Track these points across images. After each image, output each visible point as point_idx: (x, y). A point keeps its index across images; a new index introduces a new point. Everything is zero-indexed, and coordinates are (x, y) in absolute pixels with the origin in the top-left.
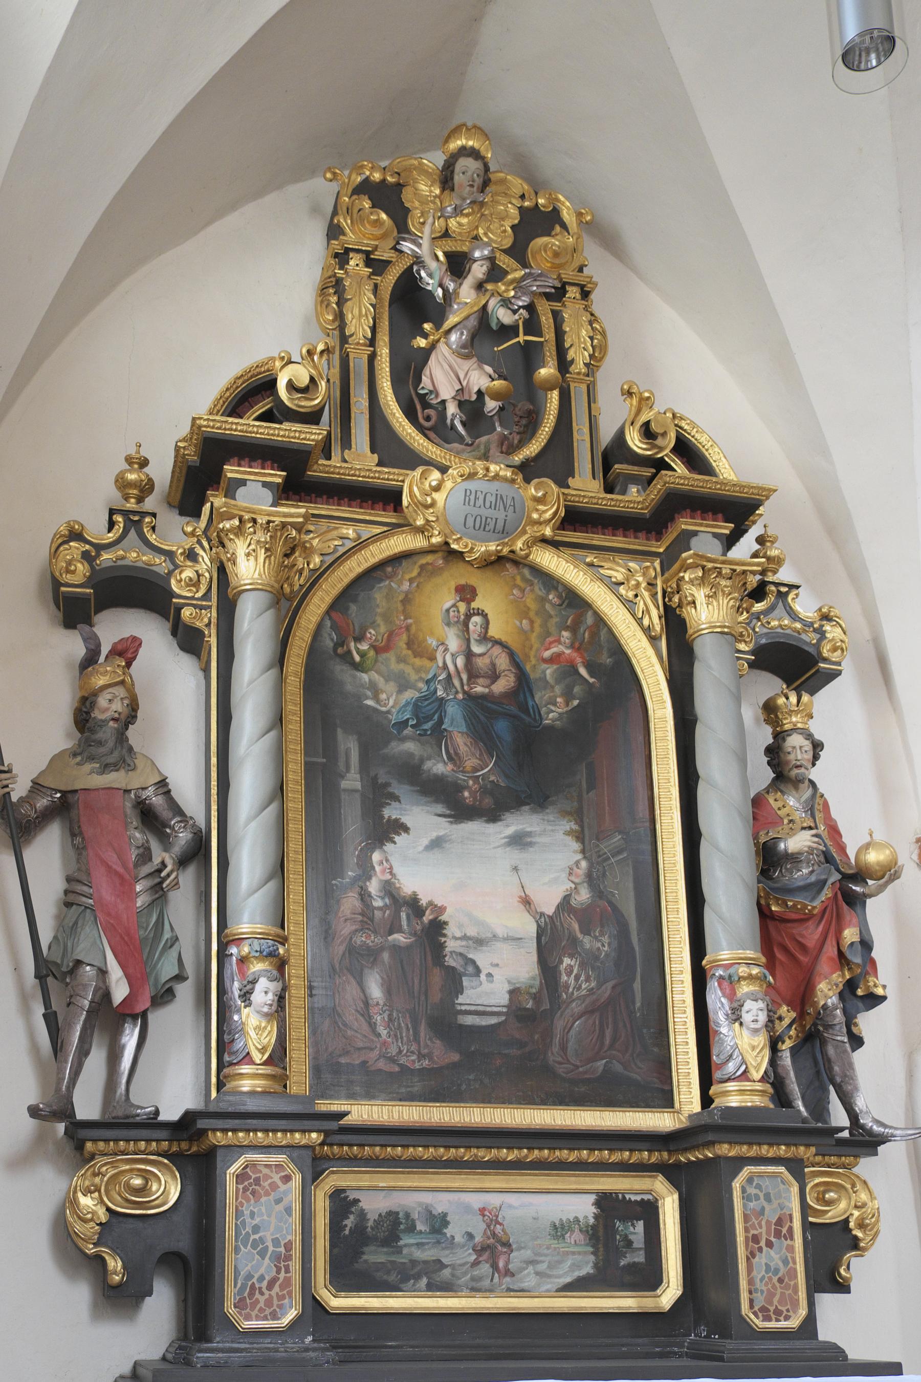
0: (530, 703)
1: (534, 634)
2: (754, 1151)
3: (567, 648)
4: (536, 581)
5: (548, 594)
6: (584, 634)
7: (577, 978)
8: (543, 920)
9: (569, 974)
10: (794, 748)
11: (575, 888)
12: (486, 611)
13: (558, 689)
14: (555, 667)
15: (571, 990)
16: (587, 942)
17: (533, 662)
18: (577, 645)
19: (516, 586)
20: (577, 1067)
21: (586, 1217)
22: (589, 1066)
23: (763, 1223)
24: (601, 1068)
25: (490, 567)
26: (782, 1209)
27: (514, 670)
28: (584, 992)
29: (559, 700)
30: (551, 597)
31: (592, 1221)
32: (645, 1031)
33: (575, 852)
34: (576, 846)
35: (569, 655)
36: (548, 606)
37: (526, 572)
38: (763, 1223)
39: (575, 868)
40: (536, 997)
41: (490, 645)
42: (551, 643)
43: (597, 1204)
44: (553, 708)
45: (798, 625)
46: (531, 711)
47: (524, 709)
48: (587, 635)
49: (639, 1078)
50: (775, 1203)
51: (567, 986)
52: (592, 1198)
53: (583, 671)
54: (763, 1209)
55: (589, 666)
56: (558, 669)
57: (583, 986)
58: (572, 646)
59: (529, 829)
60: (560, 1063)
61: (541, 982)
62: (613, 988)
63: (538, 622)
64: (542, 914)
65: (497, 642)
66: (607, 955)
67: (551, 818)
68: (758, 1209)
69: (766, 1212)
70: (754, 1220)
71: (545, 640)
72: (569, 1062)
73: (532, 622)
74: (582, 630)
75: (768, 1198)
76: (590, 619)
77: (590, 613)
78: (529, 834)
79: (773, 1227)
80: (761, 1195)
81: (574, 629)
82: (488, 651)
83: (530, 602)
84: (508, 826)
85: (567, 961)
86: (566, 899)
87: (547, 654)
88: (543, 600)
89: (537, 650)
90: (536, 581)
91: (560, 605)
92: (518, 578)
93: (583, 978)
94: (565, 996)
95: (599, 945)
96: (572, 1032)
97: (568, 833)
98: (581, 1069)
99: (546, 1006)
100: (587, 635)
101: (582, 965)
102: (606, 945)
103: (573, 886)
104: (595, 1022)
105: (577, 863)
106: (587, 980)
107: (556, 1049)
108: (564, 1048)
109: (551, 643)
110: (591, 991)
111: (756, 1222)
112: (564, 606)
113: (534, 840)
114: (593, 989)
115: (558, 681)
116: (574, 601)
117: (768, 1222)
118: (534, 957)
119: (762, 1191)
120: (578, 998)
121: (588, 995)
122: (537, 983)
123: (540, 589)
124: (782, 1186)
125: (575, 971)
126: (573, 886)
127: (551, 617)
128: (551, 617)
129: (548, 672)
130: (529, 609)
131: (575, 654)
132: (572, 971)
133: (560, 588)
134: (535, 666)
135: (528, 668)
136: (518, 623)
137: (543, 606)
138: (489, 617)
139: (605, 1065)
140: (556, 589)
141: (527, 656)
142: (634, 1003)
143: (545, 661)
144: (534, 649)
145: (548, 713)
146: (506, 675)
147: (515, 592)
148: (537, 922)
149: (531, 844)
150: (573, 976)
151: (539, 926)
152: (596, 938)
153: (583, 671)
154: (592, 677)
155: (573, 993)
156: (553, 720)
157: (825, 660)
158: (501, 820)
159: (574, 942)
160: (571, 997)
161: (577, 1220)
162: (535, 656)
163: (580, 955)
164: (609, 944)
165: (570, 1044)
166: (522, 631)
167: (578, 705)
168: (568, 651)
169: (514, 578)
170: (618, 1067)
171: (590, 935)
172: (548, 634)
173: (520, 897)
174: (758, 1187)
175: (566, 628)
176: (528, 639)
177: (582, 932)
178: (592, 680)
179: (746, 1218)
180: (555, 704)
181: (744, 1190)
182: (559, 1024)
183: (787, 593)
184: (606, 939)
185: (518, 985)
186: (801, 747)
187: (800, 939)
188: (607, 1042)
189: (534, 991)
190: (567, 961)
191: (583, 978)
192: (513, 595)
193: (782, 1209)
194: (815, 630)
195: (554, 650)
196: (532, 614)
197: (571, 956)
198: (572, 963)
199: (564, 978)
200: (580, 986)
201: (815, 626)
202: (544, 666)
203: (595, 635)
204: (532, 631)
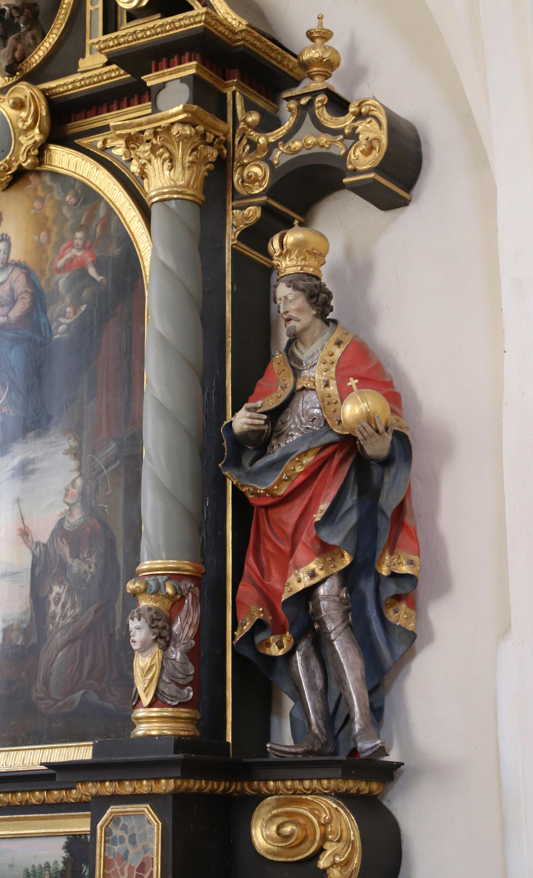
0: (43, 320)
1: (51, 245)
2: (128, 788)
3: (79, 250)
4: (55, 185)
5: (65, 196)
6: (96, 228)
7: (64, 606)
8: (38, 549)
9: (56, 604)
10: (281, 299)
11: (70, 510)
12: (9, 235)
13: (68, 299)
14: (67, 274)
15: (57, 619)
16: (75, 565)
17: (48, 273)
18: (88, 244)
19: (37, 198)
20: (56, 701)
21: (56, 862)
22: (68, 698)
23: (126, 869)
24: (78, 700)
25: (15, 185)
26: (145, 852)
27: (30, 291)
28: (69, 620)
29: (69, 310)
30: (68, 198)
31: (61, 866)
32: (122, 654)
33: (72, 471)
34: (73, 464)
35: (81, 257)
36: (65, 210)
37: (47, 178)
38: (126, 869)
39: (71, 488)
40: (26, 633)
41: (10, 270)
42: (65, 249)
43: (68, 847)
44: (62, 320)
45: (324, 139)
46: (43, 329)
47: (37, 328)
48: (98, 230)
49: (112, 706)
50: (140, 846)
51: (54, 617)
52: (63, 841)
53: (92, 271)
54: (127, 852)
55: (97, 264)
56: (69, 276)
57: (69, 614)
58: (84, 247)
59: (32, 456)
60: (42, 699)
61: (31, 615)
62: (96, 611)
63: (55, 229)
64: (38, 544)
65: (17, 265)
66: (93, 577)
67: (53, 439)
68: (122, 853)
69: (130, 857)
70: (117, 866)
71: (59, 248)
72: (50, 697)
73: (49, 232)
74: (94, 225)
75: (133, 841)
76: (102, 211)
77: (103, 204)
78: (32, 461)
79: (135, 873)
80: (126, 837)
81: (86, 228)
82: (9, 275)
83: (49, 212)
84: (14, 457)
85: (56, 589)
86: (61, 522)
87: (60, 263)
88: (60, 204)
89: (53, 261)
90: (55, 185)
91: (76, 204)
92: (39, 188)
93: (68, 605)
94: (51, 627)
95: (86, 567)
96: (55, 665)
97: (67, 453)
98: (60, 704)
99: (34, 640)
100: (98, 230)
101: (70, 592)
102: (93, 566)
103: (67, 508)
104: (76, 652)
105: (74, 481)
106: (73, 607)
107: (39, 684)
108: (46, 683)
109: (65, 249)
110: (75, 618)
111: (118, 868)
112: (79, 204)
113: (35, 466)
114: (77, 615)
115: (69, 289)
116: (89, 196)
117: (131, 868)
118: (27, 591)
119: (127, 833)
120: (63, 627)
121: (73, 623)
122: (29, 616)
123: (59, 193)
124: (148, 826)
125: (63, 600)
126: (67, 508)
127: (66, 220)
128: (66, 220)
129: (61, 282)
130: (47, 218)
131: (87, 255)
132: (60, 599)
133: (77, 186)
134: (49, 279)
135: (43, 284)
136: (36, 237)
137: (61, 211)
138: (12, 240)
139: (82, 698)
140: (73, 187)
141: (43, 272)
142: (114, 625)
143: (59, 271)
144: (49, 262)
145: (57, 327)
146: (23, 298)
147: (35, 205)
148: (33, 552)
149: (33, 472)
150: (60, 605)
151: (34, 556)
152: (84, 559)
153: (92, 271)
154: (100, 274)
155: (59, 623)
156: (61, 334)
157: (355, 172)
158: (8, 453)
159: (64, 566)
160: (57, 627)
161: (48, 865)
162: (50, 269)
163: (68, 580)
164: (96, 565)
165: (52, 677)
166: (40, 247)
167: (86, 310)
168: (79, 254)
169: (35, 190)
170: (94, 697)
171: (78, 557)
172: (63, 240)
173: (20, 529)
174: (125, 828)
175: (80, 228)
176: (44, 251)
177: (71, 556)
178: (99, 278)
179: (107, 863)
180: (64, 316)
181: (108, 833)
182: (44, 657)
183: (311, 103)
184: (93, 560)
185: (11, 623)
186: (286, 297)
187: (280, 525)
188: (86, 671)
189: (24, 626)
190: (56, 589)
191: (68, 605)
192: (34, 208)
193: (145, 852)
194: (346, 137)
195: (68, 256)
196: (50, 223)
197: (60, 584)
198: (61, 591)
199: (53, 607)
200: (66, 614)
201: (347, 131)
202: (59, 276)
203: (106, 226)
204: (49, 241)
